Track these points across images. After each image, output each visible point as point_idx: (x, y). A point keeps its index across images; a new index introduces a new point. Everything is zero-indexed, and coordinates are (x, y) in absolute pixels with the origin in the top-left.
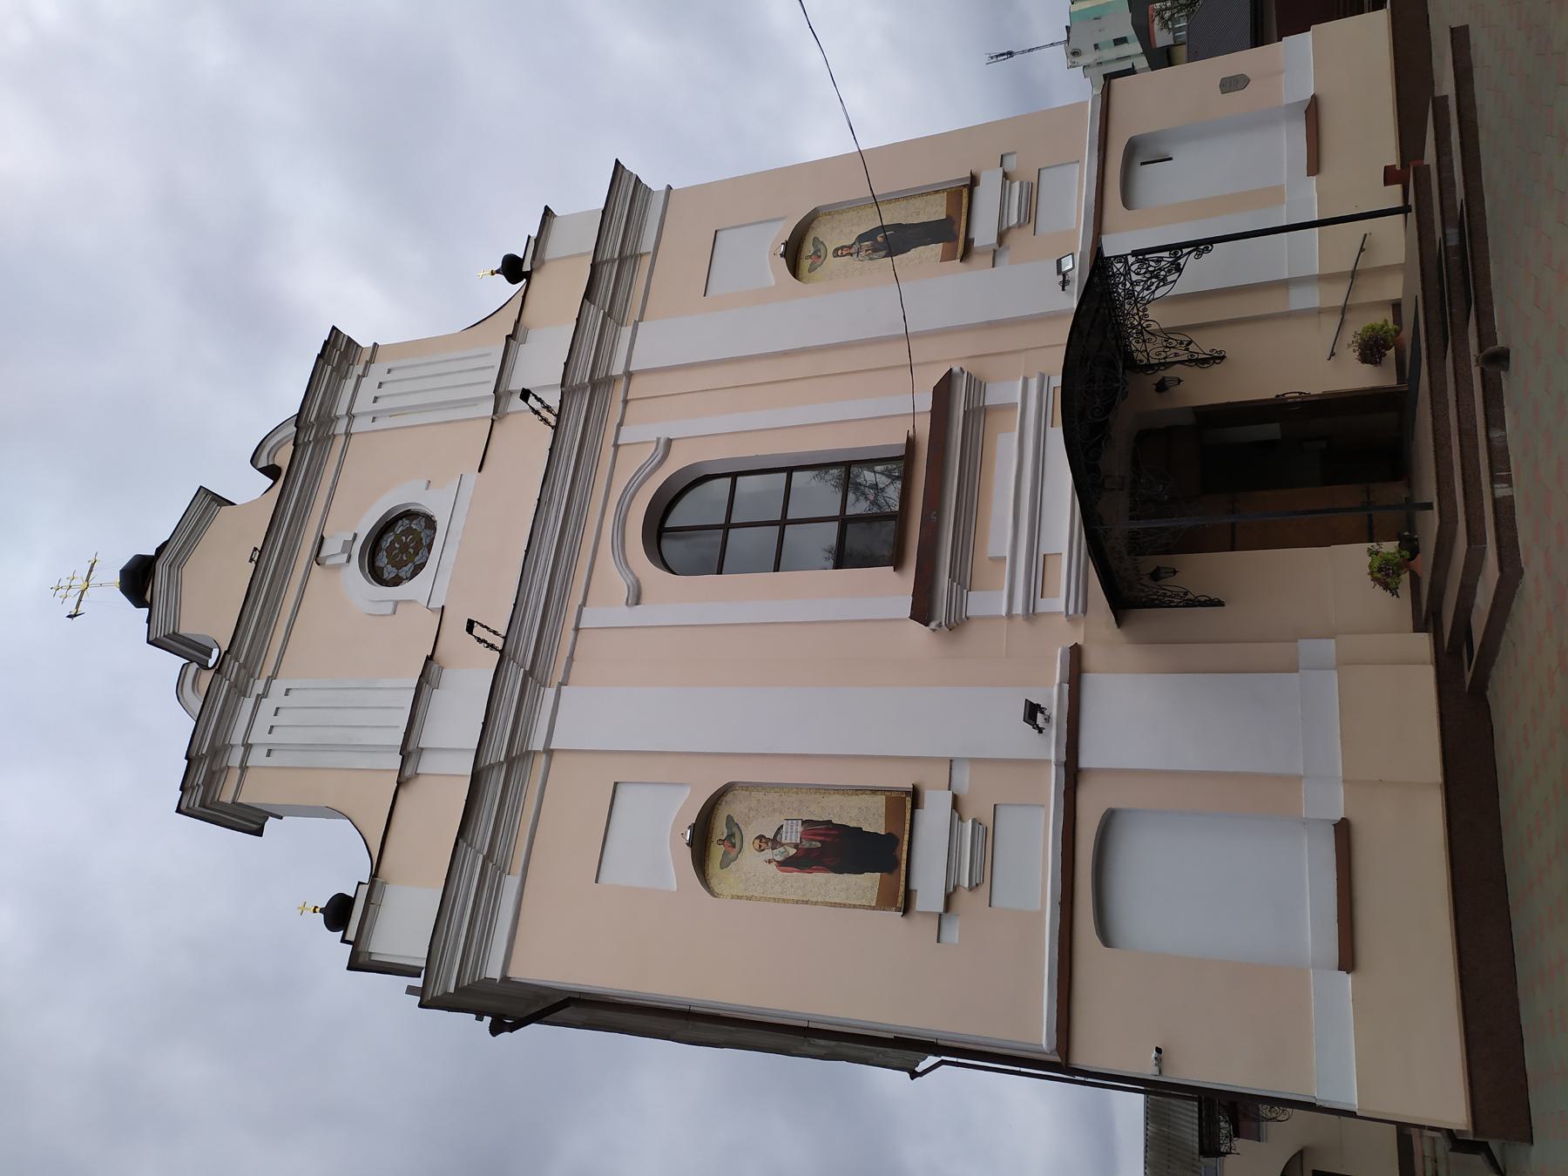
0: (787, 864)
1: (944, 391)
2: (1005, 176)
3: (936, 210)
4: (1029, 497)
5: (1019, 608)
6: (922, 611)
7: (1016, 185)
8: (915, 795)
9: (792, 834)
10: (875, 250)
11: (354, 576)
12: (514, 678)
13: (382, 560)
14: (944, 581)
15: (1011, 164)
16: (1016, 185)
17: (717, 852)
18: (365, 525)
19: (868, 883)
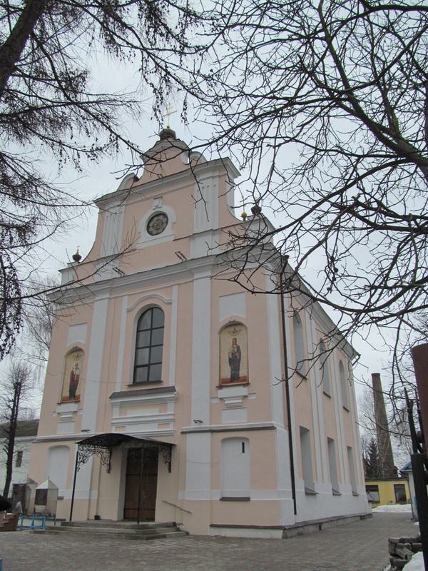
0: (72, 372)
1: (172, 389)
2: (245, 397)
3: (242, 373)
4: (140, 422)
5: (114, 421)
6: (114, 396)
7: (240, 401)
9: (77, 373)
10: (233, 354)
11: (150, 213)
15: (253, 397)
16: (240, 401)
19: (67, 394)
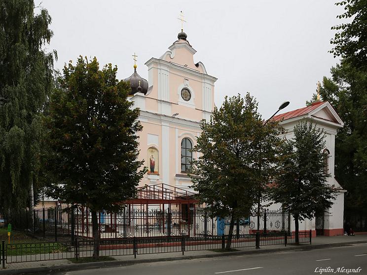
6: (177, 175)
8: (158, 175)
9: (153, 160)
12: (171, 120)
13: (184, 90)
14: (180, 178)
17: (151, 149)
18: (189, 88)
